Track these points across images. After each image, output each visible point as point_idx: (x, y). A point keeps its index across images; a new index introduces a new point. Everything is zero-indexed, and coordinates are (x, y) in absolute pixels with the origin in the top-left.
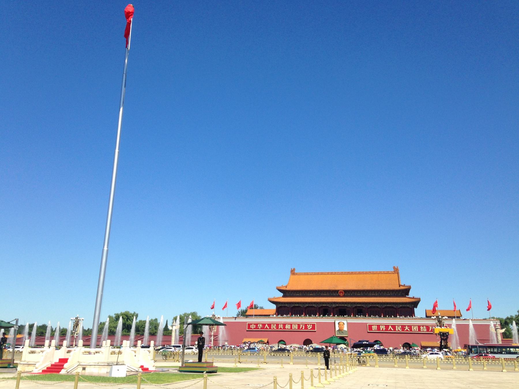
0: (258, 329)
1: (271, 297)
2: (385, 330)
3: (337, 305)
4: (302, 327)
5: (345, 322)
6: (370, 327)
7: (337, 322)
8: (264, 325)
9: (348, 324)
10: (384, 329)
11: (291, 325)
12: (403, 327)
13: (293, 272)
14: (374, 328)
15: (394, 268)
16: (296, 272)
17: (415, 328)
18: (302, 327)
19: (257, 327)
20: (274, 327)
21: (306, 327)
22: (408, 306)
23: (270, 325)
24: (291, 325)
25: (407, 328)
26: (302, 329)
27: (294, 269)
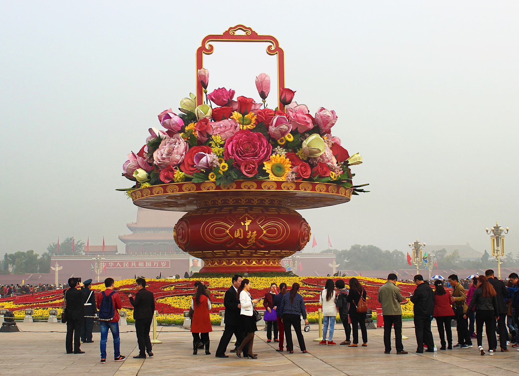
0: (110, 267)
1: (122, 234)
4: (156, 265)
11: (145, 263)
18: (156, 265)
20: (126, 265)
21: (160, 265)
26: (156, 266)
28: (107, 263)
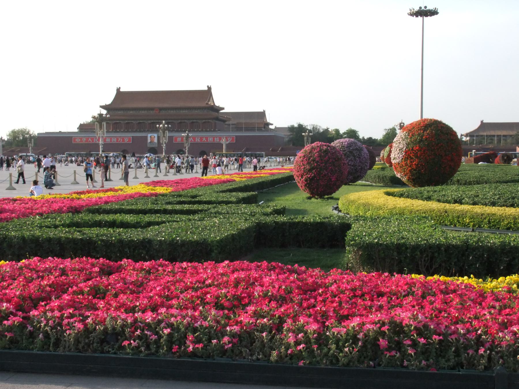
13: (118, 90)
15: (208, 86)
19: (81, 141)
21: (123, 140)
25: (204, 139)
27: (120, 88)
28: (81, 139)
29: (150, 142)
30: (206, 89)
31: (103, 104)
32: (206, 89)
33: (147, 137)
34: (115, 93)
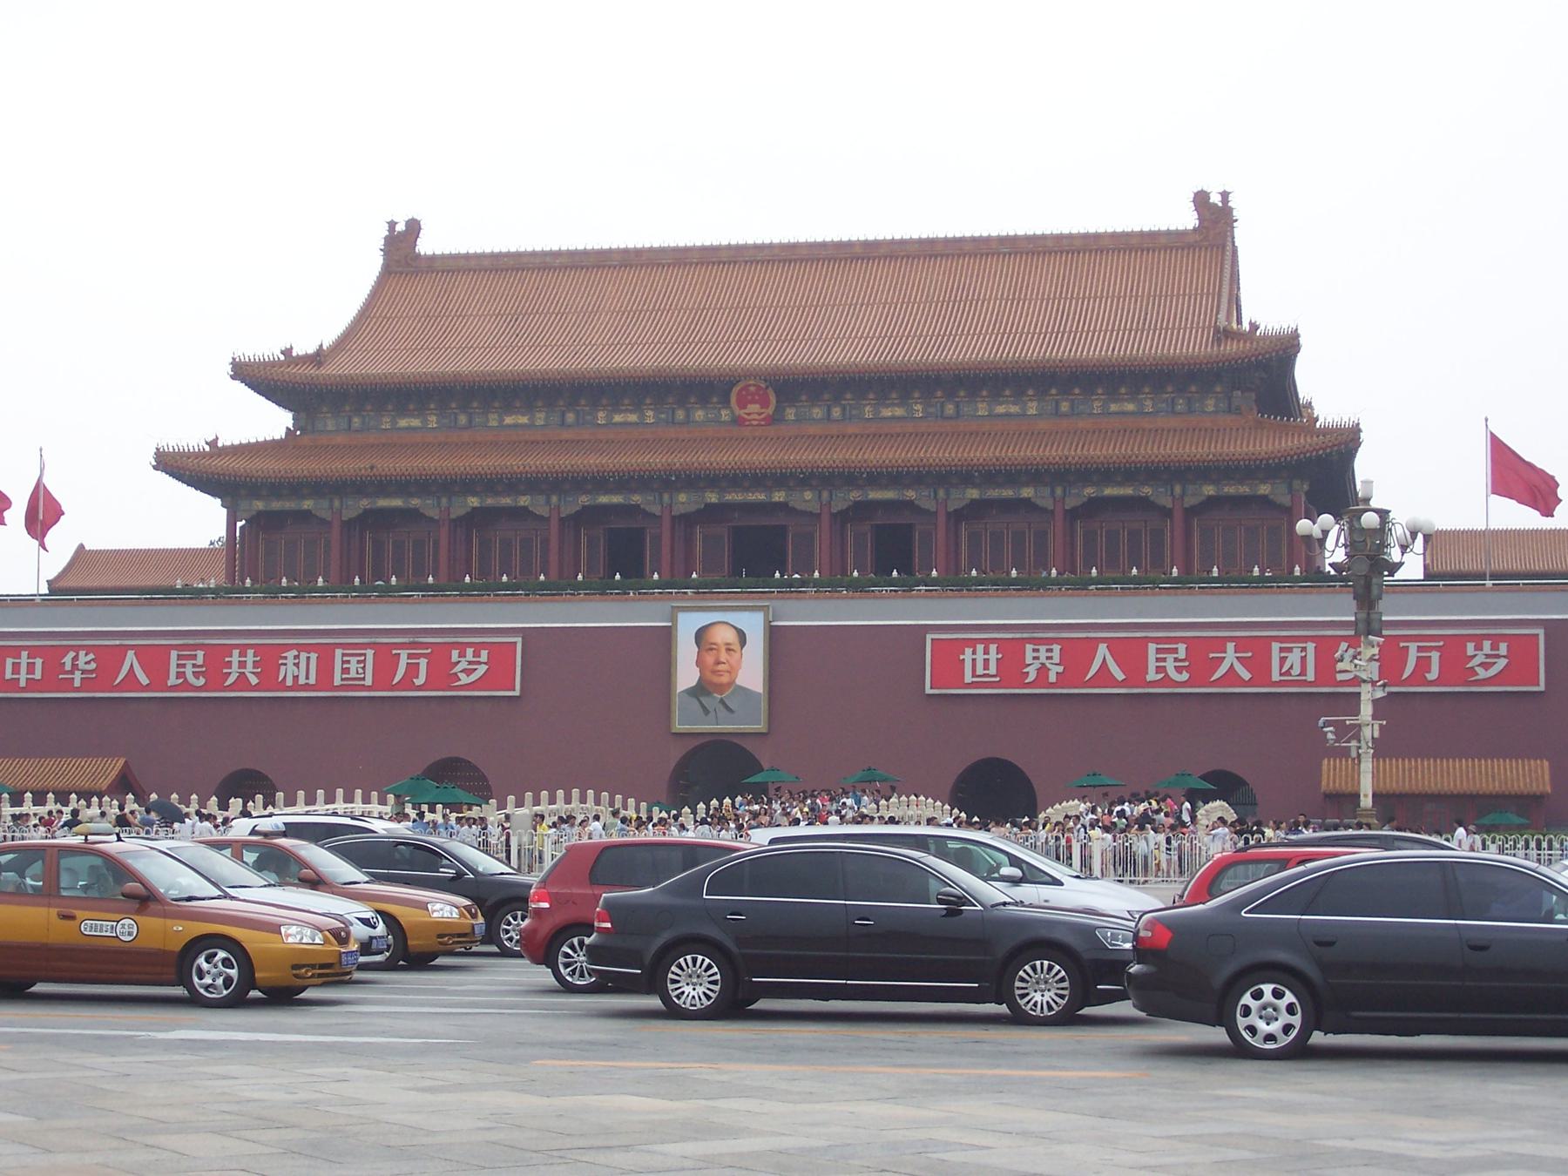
1: (191, 438)
2: (1062, 679)
3: (712, 498)
4: (413, 670)
5: (753, 624)
6: (950, 653)
7: (688, 625)
8: (109, 657)
9: (774, 636)
10: (1054, 672)
11: (325, 655)
12: (1202, 652)
13: (400, 246)
14: (979, 664)
15: (1201, 199)
16: (426, 245)
17: (1294, 658)
18: (413, 670)
21: (442, 672)
22: (1264, 489)
23: (154, 659)
24: (325, 655)
25: (1230, 656)
26: (407, 683)
27: (414, 227)
28: (52, 656)
29: (701, 690)
30: (1187, 219)
31: (265, 347)
32: (1187, 219)
33: (666, 636)
34: (376, 263)
